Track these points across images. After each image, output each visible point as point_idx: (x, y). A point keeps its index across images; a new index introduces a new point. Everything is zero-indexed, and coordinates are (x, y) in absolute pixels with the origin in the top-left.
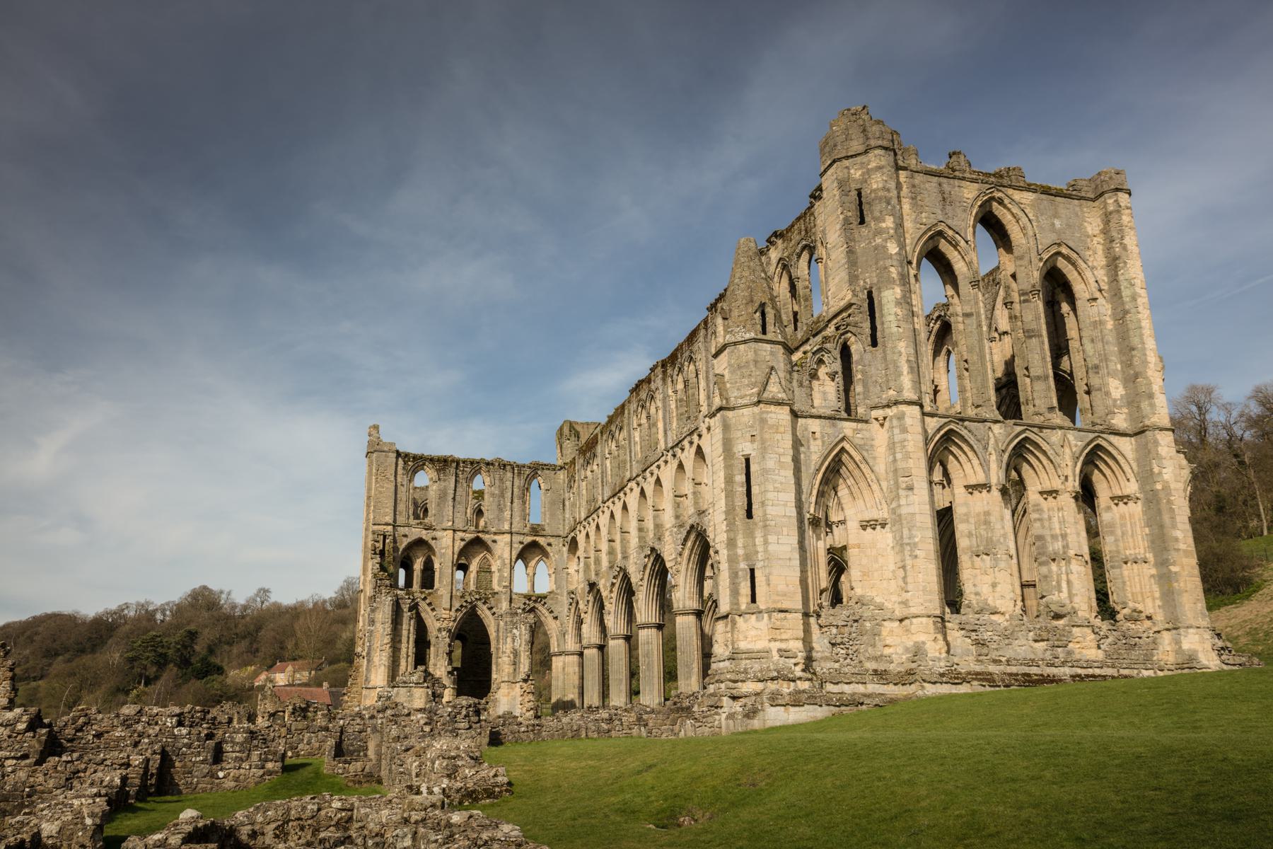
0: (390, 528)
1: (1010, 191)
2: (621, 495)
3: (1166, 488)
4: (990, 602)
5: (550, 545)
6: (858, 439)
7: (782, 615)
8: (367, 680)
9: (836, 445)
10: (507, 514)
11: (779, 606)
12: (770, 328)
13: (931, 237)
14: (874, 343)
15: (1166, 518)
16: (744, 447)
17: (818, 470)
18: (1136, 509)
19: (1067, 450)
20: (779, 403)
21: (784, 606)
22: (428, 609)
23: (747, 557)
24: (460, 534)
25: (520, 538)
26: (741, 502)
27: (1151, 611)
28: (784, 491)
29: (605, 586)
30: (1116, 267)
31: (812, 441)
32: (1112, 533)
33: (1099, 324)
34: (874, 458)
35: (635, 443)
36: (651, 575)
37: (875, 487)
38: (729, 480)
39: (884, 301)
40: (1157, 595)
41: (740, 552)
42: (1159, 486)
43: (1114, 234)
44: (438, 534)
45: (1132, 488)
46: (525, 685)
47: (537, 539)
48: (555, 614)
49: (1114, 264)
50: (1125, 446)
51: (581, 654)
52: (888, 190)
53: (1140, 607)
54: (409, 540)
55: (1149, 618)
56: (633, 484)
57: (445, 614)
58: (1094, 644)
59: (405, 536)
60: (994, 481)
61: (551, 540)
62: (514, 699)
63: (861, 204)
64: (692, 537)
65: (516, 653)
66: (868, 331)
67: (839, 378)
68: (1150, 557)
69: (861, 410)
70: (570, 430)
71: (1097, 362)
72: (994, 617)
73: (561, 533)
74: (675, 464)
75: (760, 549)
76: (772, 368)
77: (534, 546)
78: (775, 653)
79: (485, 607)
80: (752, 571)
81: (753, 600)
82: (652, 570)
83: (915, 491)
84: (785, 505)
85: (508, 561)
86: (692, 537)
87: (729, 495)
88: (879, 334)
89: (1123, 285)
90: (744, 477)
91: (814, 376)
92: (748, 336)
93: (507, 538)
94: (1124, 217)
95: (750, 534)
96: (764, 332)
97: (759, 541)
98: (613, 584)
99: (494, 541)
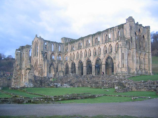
2: (81, 50)
3: (150, 58)
8: (44, 71)
16: (123, 52)
24: (51, 52)
26: (122, 57)
29: (75, 61)
38: (121, 55)
41: (122, 62)
50: (147, 54)
56: (84, 49)
69: (130, 49)
74: (94, 48)
77: (60, 54)
87: (121, 56)
95: (123, 60)
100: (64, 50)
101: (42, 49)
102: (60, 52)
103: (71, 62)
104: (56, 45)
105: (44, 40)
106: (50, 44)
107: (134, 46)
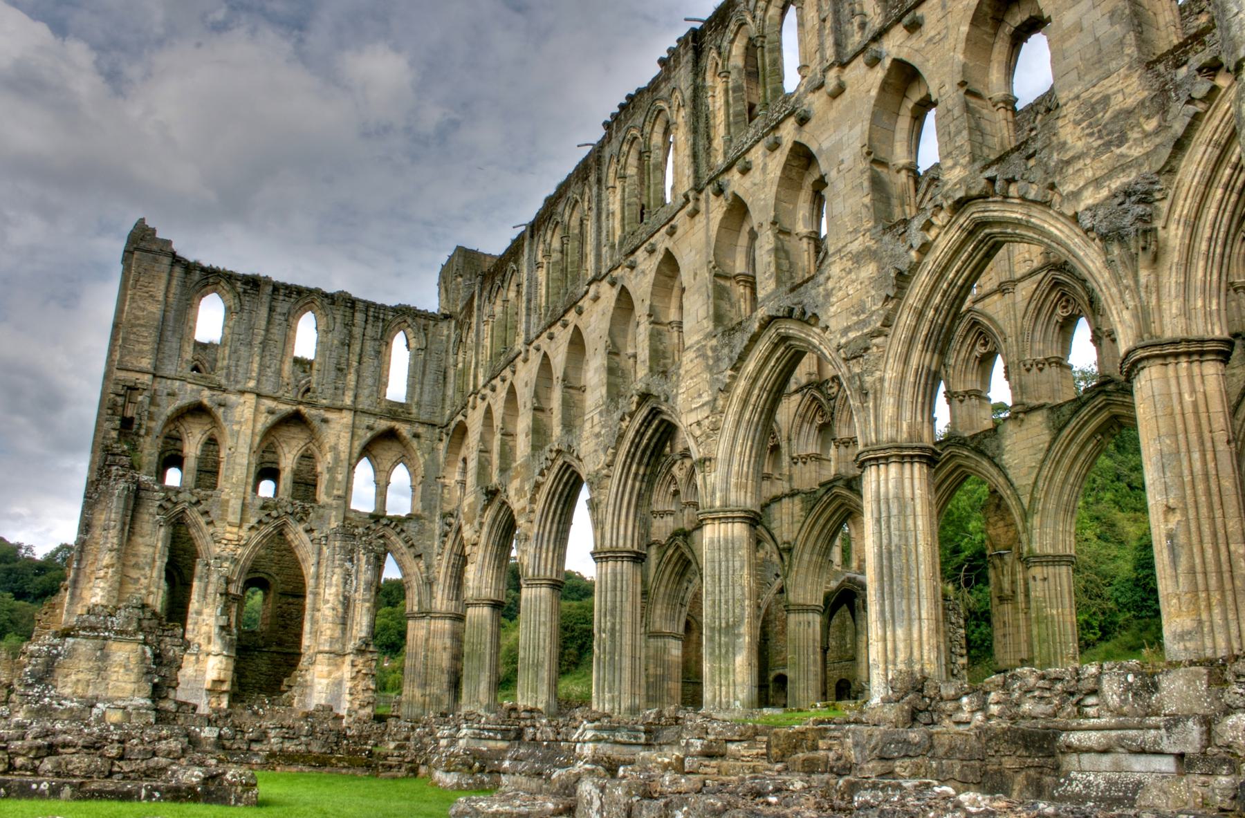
5: (416, 436)
10: (352, 378)
22: (202, 521)
24: (269, 403)
25: (370, 421)
29: (520, 491)
35: (610, 214)
36: (630, 456)
46: (360, 661)
48: (420, 550)
51: (459, 618)
57: (231, 533)
59: (172, 394)
61: (421, 430)
62: (339, 683)
64: (762, 347)
65: (347, 603)
70: (466, 259)
73: (437, 420)
77: (391, 435)
79: (300, 528)
82: (635, 444)
85: (344, 456)
86: (762, 347)
93: (347, 417)
98: (537, 486)
99: (325, 421)
100: (450, 392)
101: (146, 363)
102: (395, 411)
103: (490, 513)
104: (349, 325)
106: (264, 312)
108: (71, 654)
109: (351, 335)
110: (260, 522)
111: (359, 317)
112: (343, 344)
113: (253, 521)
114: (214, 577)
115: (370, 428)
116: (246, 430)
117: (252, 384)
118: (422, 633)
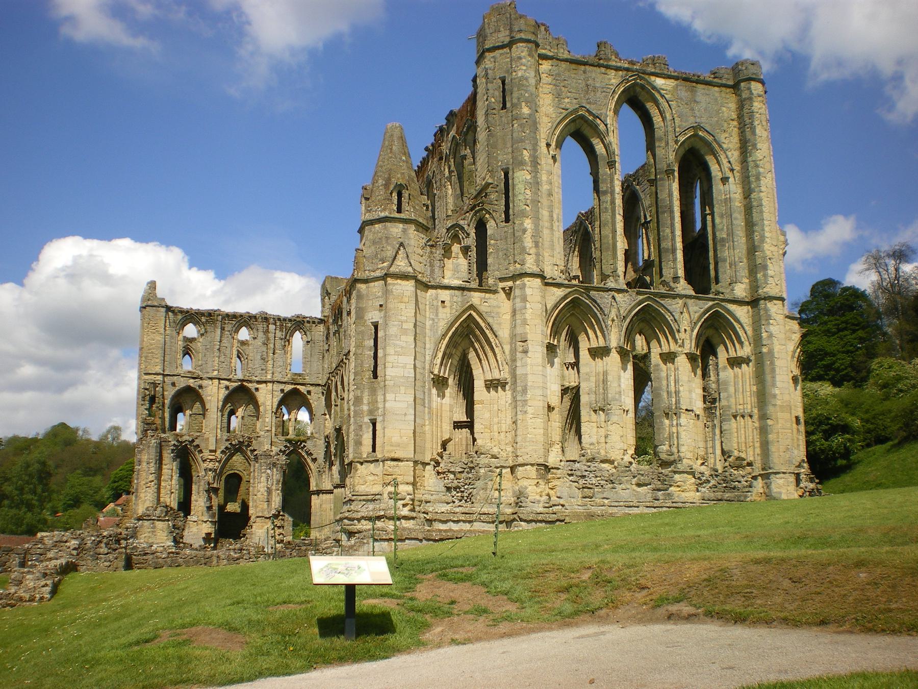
0: (160, 378)
1: (653, 78)
4: (603, 452)
6: (483, 308)
7: (395, 463)
9: (464, 312)
11: (393, 455)
12: (405, 206)
13: (573, 121)
14: (507, 220)
15: (768, 378)
17: (444, 336)
18: (747, 370)
19: (686, 315)
20: (404, 277)
21: (396, 456)
23: (371, 412)
25: (282, 386)
26: (369, 363)
27: (752, 459)
28: (404, 354)
30: (746, 149)
31: (441, 309)
32: (726, 390)
33: (728, 201)
34: (500, 324)
37: (497, 350)
39: (516, 181)
40: (757, 445)
42: (765, 350)
43: (748, 121)
44: (205, 383)
45: (746, 351)
47: (298, 387)
48: (314, 457)
49: (745, 147)
50: (742, 313)
52: (526, 79)
53: (743, 455)
54: (177, 388)
55: (750, 464)
58: (694, 487)
60: (613, 344)
61: (311, 388)
63: (504, 91)
65: (269, 491)
66: (503, 208)
67: (473, 253)
68: (756, 411)
69: (491, 281)
71: (725, 236)
72: (603, 465)
73: (320, 383)
75: (380, 405)
76: (402, 244)
77: (295, 392)
78: (386, 495)
80: (374, 425)
81: (374, 450)
83: (529, 354)
84: (404, 367)
88: (511, 212)
89: (751, 164)
90: (372, 342)
91: (447, 253)
92: (383, 215)
94: (755, 104)
95: (373, 392)
96: (399, 210)
97: (380, 398)
99: (257, 389)
105: (169, 309)
106: (219, 331)
107: (523, 250)
108: (142, 526)
109: (268, 339)
110: (226, 448)
111: (272, 327)
112: (264, 344)
113: (223, 448)
114: (202, 483)
115: (282, 391)
116: (215, 399)
117: (216, 373)
118: (318, 502)
